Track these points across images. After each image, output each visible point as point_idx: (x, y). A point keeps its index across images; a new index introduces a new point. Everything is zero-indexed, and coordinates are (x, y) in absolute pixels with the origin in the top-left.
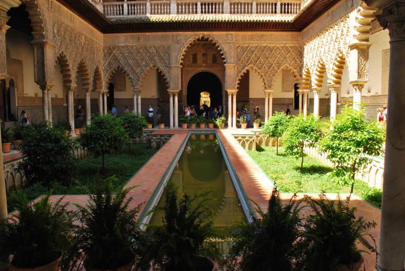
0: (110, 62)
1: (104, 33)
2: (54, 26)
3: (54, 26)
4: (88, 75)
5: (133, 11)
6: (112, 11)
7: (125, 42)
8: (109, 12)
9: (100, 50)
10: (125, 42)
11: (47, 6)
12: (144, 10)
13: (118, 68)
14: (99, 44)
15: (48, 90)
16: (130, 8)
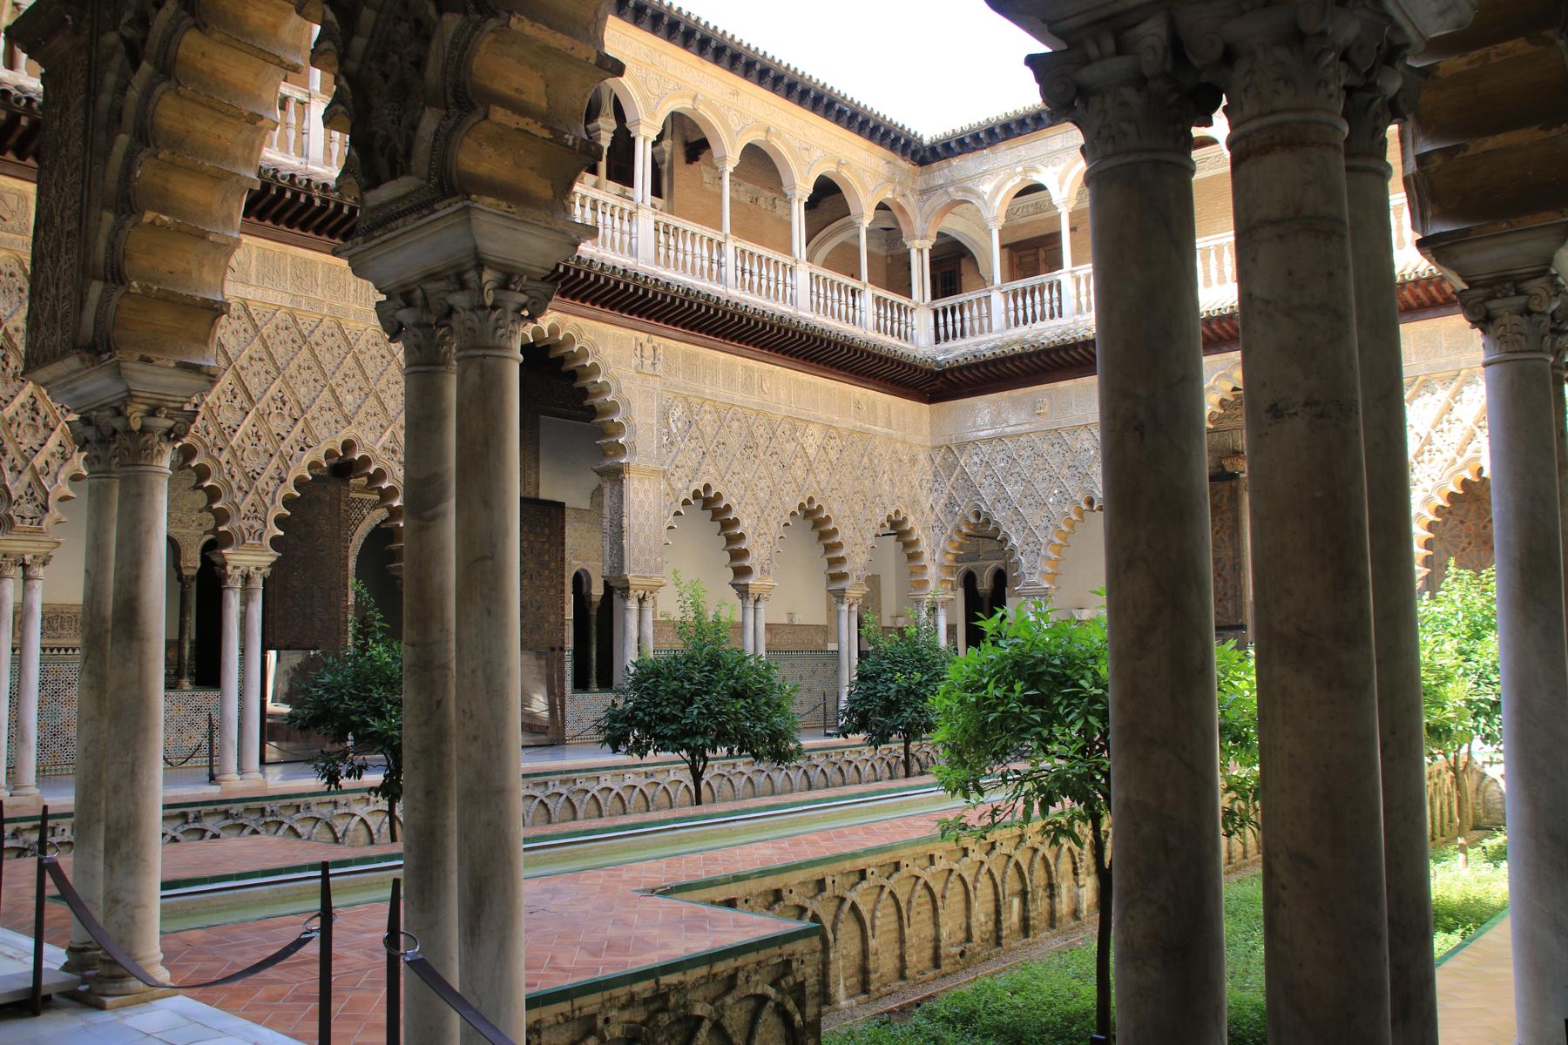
0: (950, 497)
1: (930, 401)
2: (665, 415)
3: (665, 415)
4: (839, 545)
5: (1021, 313)
6: (958, 326)
7: (993, 424)
8: (950, 328)
9: (913, 461)
10: (993, 424)
11: (635, 362)
12: (1056, 304)
13: (978, 515)
14: (904, 442)
15: (641, 601)
16: (1011, 305)
